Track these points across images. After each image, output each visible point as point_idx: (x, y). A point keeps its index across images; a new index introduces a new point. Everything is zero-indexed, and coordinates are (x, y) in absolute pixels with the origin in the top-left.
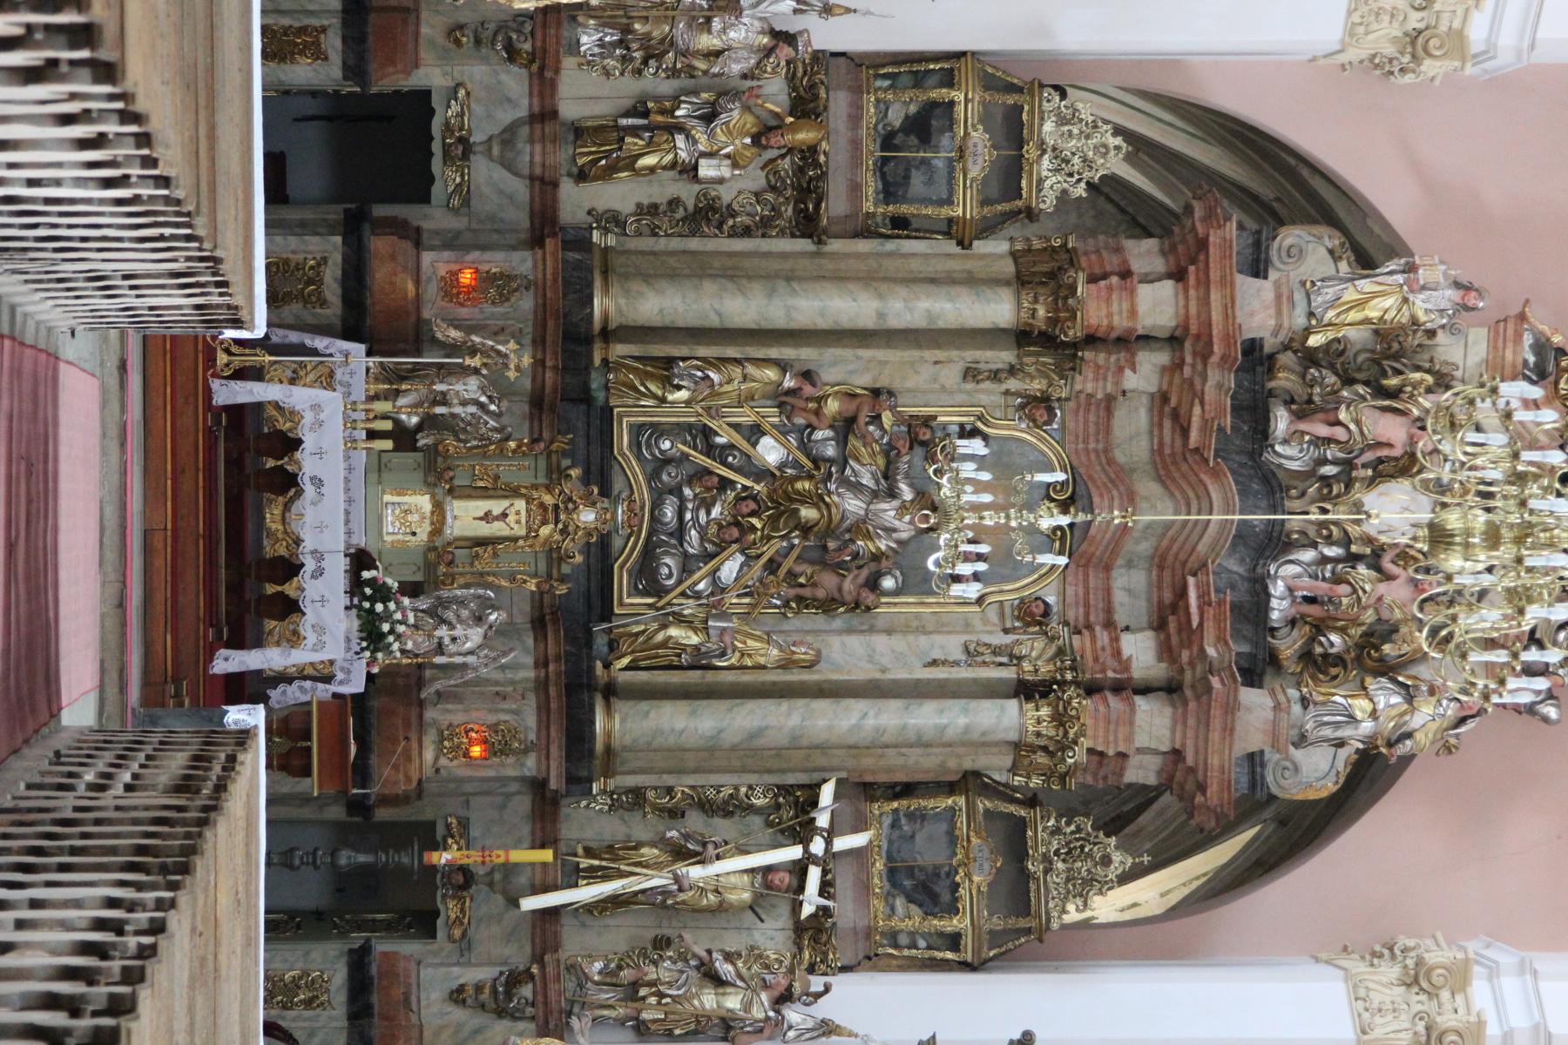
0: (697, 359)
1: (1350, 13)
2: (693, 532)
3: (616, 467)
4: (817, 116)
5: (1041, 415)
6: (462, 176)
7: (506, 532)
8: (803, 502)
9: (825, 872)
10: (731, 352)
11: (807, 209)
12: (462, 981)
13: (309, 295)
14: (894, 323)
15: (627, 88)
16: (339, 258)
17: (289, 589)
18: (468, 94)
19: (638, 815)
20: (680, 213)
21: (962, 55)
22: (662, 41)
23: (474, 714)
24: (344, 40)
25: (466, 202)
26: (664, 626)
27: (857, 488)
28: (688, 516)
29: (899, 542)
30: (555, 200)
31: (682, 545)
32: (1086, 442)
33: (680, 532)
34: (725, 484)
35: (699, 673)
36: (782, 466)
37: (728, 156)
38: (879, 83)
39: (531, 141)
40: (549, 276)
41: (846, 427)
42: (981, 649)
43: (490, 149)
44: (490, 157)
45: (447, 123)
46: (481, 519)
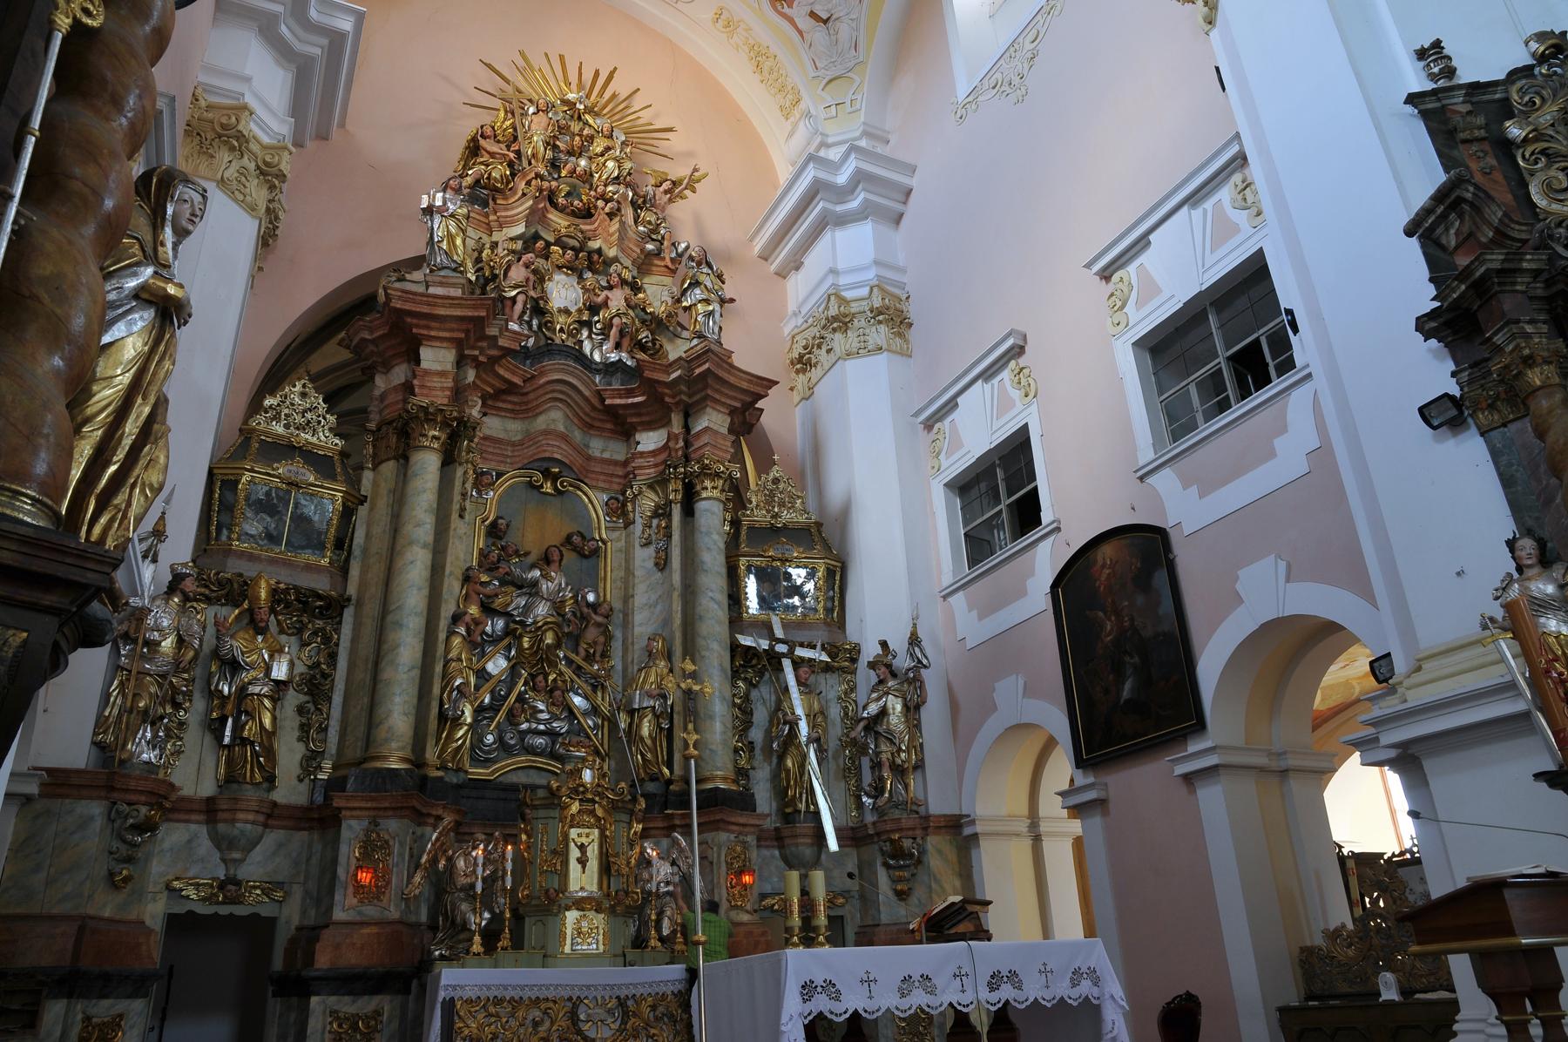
0: (442, 694)
1: (235, 200)
2: (554, 725)
3: (501, 779)
4: (246, 583)
5: (486, 479)
6: (255, 887)
7: (596, 845)
8: (541, 640)
9: (802, 645)
10: (439, 668)
11: (320, 607)
12: (890, 894)
13: (368, 1027)
14: (430, 539)
15: (194, 738)
16: (333, 999)
17: (982, 1023)
18: (177, 879)
19: (751, 773)
20: (311, 706)
21: (211, 474)
22: (160, 686)
23: (722, 881)
24: (104, 996)
25: (279, 885)
26: (642, 739)
27: (527, 609)
28: (542, 727)
29: (567, 585)
30: (287, 807)
31: (562, 734)
32: (507, 456)
33: (551, 734)
34: (521, 698)
35: (675, 716)
36: (508, 659)
37: (271, 656)
38: (224, 538)
39: (233, 821)
40: (369, 805)
41: (488, 610)
42: (646, 536)
43: (235, 861)
44: (242, 860)
45: (203, 900)
46: (584, 867)
